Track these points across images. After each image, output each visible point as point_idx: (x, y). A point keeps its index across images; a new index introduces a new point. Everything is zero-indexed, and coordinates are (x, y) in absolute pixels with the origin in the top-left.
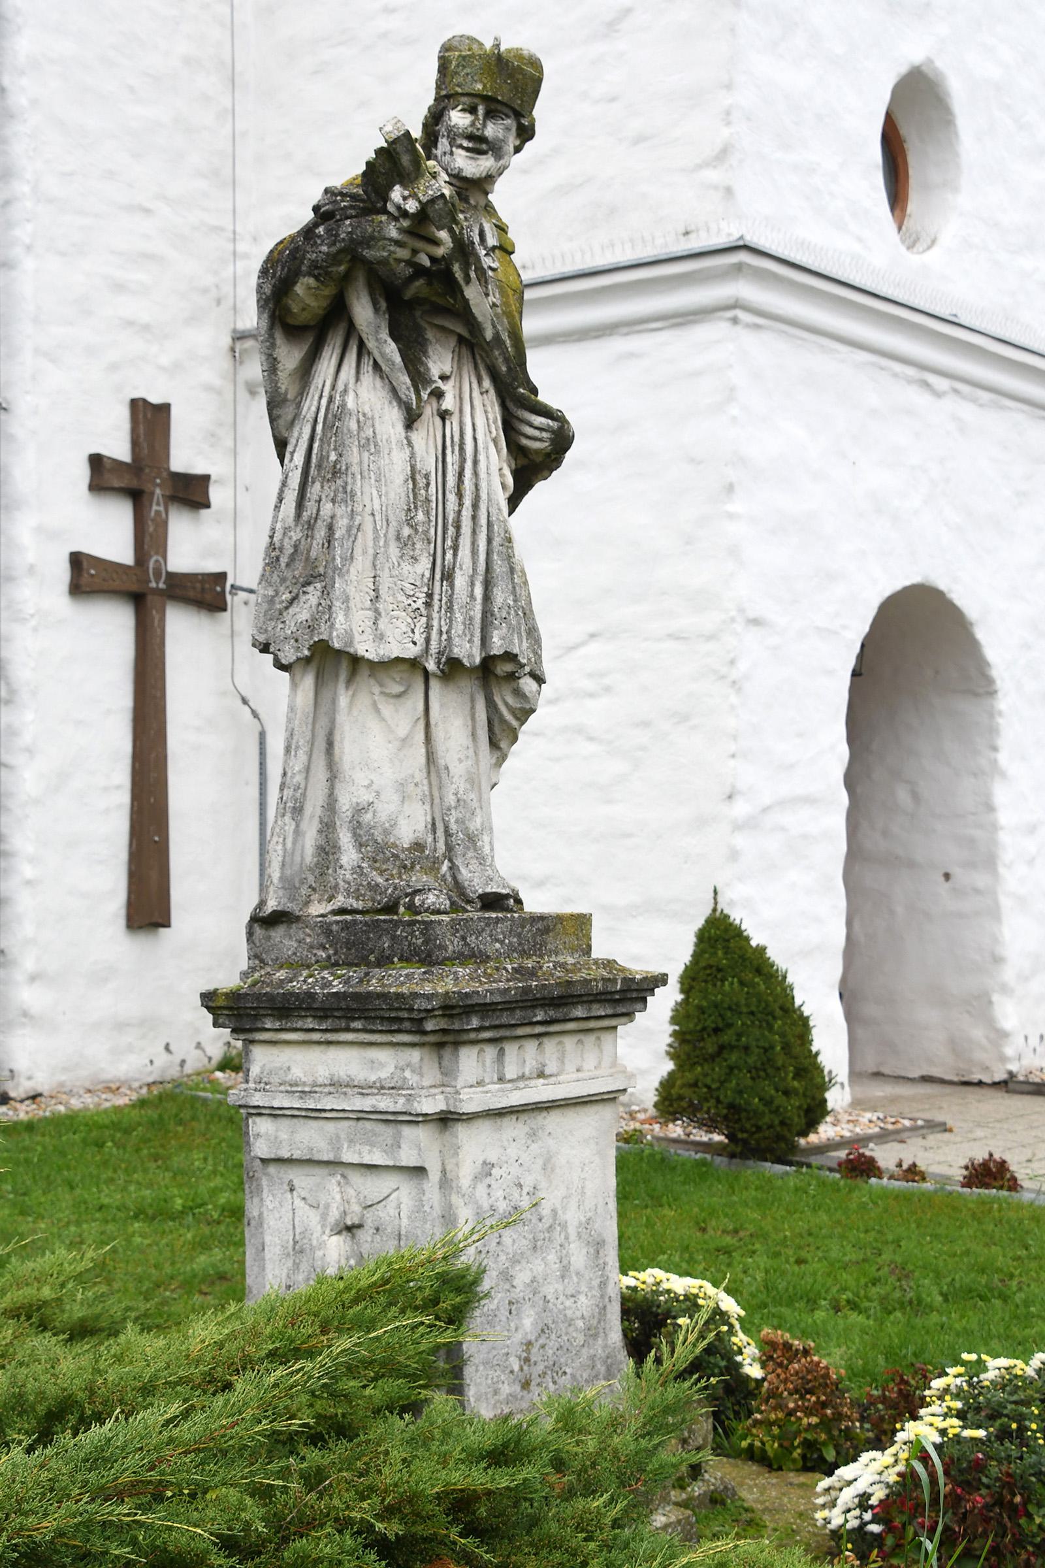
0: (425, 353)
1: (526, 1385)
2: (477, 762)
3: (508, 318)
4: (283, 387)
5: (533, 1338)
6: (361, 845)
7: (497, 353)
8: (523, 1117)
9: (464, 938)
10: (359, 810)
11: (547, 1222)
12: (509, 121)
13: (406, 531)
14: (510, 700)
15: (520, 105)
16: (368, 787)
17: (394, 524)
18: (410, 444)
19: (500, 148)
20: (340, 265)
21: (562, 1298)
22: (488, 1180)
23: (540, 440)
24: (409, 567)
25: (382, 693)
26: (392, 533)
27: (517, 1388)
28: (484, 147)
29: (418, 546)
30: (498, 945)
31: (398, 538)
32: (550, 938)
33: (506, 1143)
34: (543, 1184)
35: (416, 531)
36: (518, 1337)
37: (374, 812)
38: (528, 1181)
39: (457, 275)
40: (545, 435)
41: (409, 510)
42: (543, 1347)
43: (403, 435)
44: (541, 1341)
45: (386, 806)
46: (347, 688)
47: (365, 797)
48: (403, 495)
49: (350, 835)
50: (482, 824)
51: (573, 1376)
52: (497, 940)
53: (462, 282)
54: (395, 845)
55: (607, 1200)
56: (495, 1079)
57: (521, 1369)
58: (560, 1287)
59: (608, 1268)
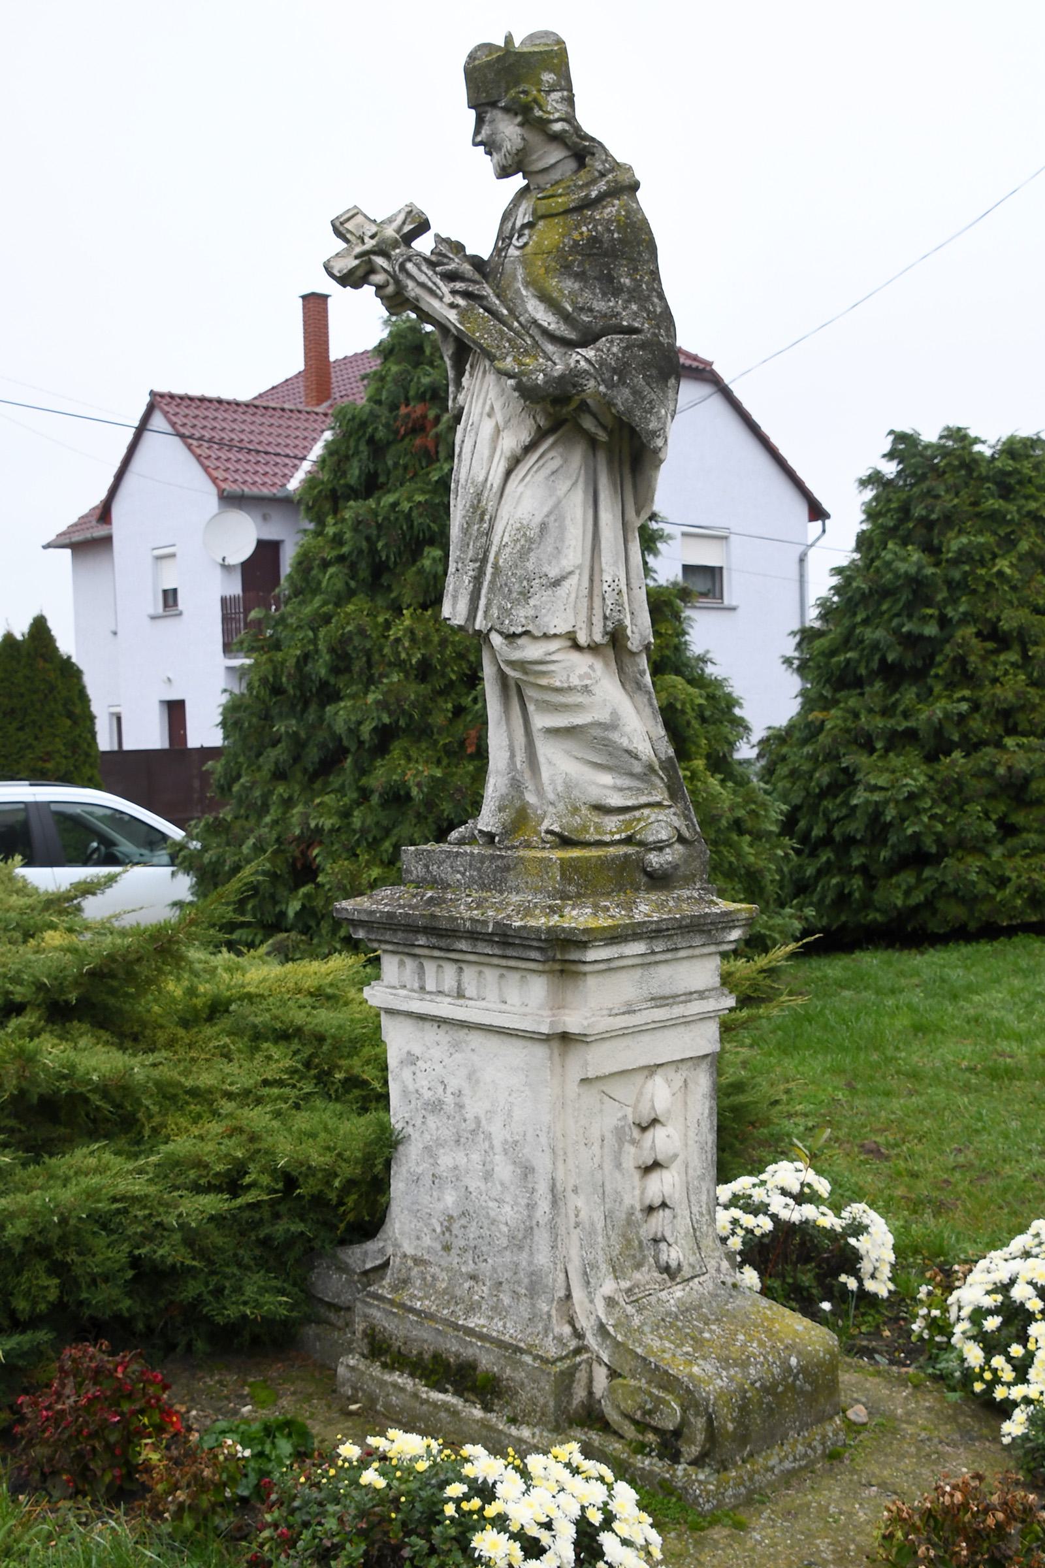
1: (447, 1248)
8: (444, 1027)
9: (426, 866)
30: (459, 876)
32: (511, 876)
34: (467, 1091)
36: (440, 1206)
38: (454, 1083)
51: (494, 1269)
58: (483, 1187)
59: (537, 1195)
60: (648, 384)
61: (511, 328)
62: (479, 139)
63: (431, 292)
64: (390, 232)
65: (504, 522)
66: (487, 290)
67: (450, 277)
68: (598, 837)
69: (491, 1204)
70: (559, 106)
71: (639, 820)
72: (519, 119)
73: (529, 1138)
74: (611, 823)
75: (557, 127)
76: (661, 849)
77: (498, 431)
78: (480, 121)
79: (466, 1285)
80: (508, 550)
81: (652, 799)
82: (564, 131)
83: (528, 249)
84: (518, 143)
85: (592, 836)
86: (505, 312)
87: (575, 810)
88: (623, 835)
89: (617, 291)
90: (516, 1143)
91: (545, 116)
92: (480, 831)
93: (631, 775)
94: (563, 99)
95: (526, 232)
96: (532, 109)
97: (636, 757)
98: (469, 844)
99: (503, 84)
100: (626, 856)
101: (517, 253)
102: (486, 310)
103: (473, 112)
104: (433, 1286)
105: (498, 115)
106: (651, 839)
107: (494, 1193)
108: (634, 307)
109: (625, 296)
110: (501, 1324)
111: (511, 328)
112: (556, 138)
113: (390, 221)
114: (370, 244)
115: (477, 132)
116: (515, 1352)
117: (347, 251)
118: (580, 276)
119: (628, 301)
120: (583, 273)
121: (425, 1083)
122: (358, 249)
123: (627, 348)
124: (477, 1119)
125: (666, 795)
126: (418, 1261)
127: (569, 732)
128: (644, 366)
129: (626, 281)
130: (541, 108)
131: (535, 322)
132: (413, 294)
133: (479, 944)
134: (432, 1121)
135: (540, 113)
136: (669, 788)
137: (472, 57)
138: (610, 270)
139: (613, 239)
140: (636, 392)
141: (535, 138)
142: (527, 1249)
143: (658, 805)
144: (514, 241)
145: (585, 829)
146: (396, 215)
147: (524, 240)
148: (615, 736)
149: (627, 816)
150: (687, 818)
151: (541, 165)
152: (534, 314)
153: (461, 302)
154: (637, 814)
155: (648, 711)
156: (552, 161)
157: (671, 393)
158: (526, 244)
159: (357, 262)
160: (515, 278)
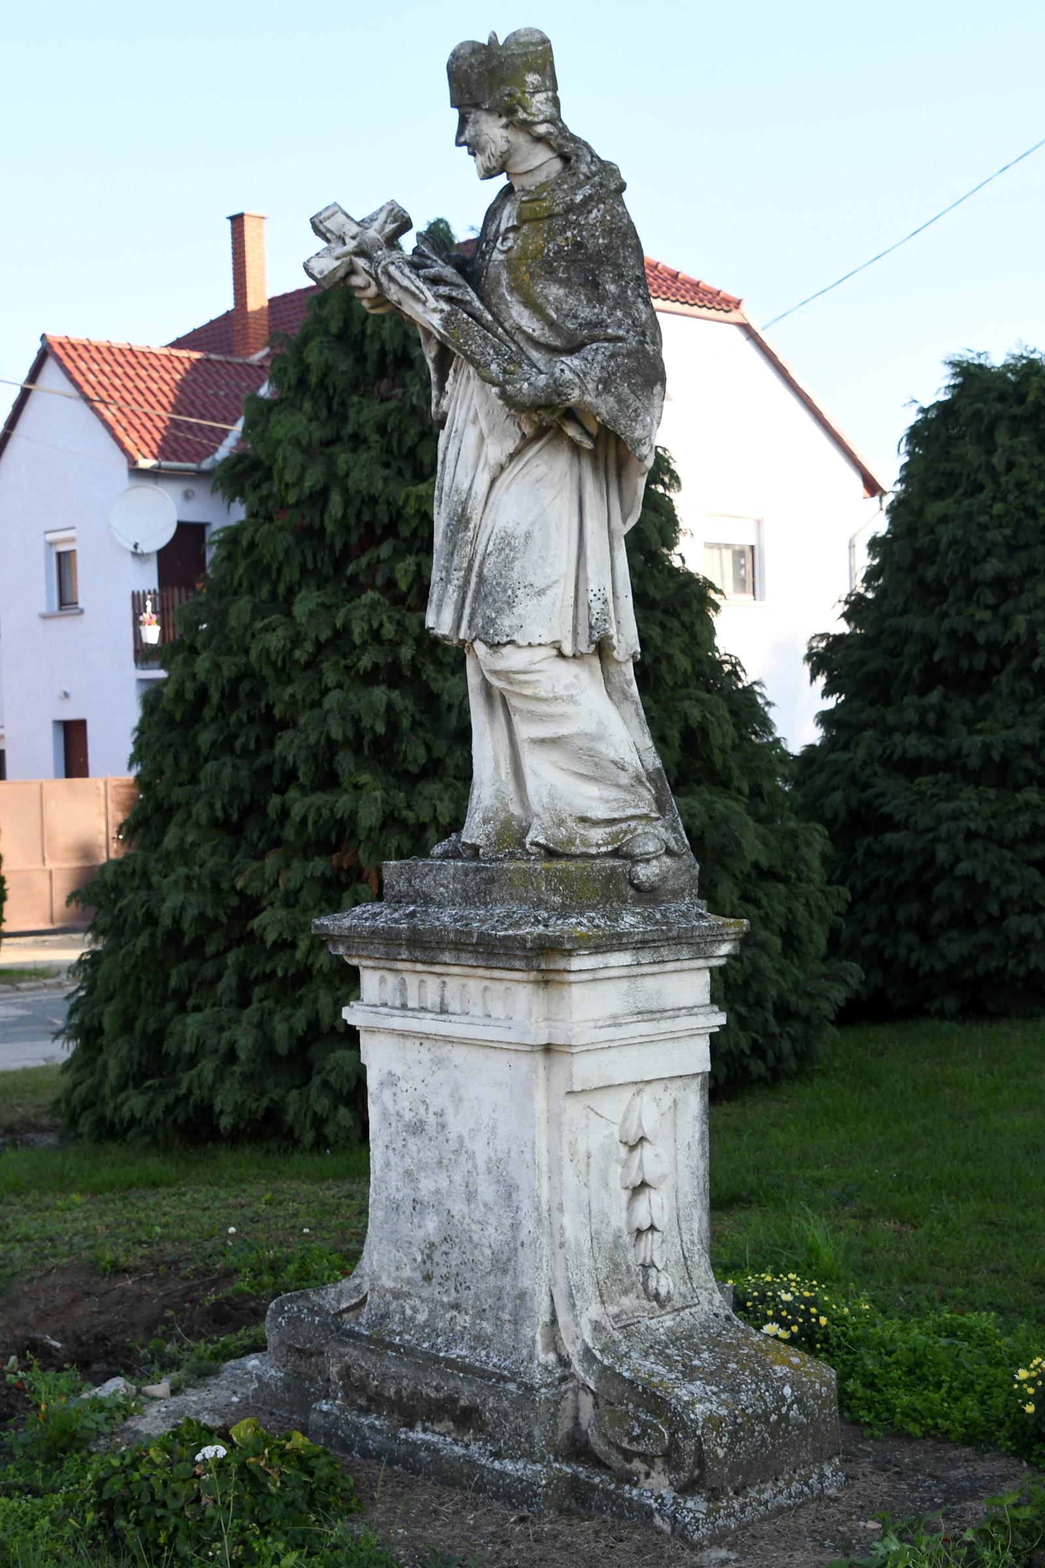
1: (428, 1278)
5: (437, 1241)
11: (454, 1145)
19: (478, 143)
21: (467, 1220)
22: (394, 1089)
27: (417, 1276)
32: (495, 888)
33: (410, 1063)
34: (450, 1111)
36: (420, 1234)
38: (436, 1104)
42: (446, 1254)
44: (445, 1248)
51: (477, 1297)
52: (442, 885)
55: (523, 1148)
56: (398, 1003)
57: (424, 1262)
58: (466, 1210)
59: (521, 1214)
60: (633, 392)
61: (495, 335)
62: (462, 139)
63: (414, 295)
64: (372, 233)
65: (488, 531)
66: (471, 296)
67: (435, 281)
68: (584, 850)
69: (474, 1227)
70: (543, 108)
71: (626, 833)
72: (504, 120)
73: (513, 1155)
74: (597, 835)
75: (542, 129)
76: (648, 861)
77: (482, 439)
78: (463, 122)
79: (448, 1316)
80: (492, 559)
81: (638, 812)
82: (551, 133)
83: (513, 254)
84: (503, 146)
85: (578, 849)
86: (490, 318)
87: (561, 823)
88: (610, 849)
89: (601, 300)
90: (500, 1160)
91: (530, 118)
92: (464, 844)
93: (618, 786)
94: (547, 99)
95: (511, 235)
96: (516, 111)
97: (623, 769)
98: (454, 858)
100: (613, 868)
101: (502, 257)
102: (470, 315)
103: (456, 111)
104: (412, 1319)
105: (483, 117)
106: (637, 851)
107: (477, 1216)
108: (619, 314)
109: (611, 303)
110: (484, 1353)
111: (495, 335)
112: (539, 139)
113: (372, 219)
115: (461, 132)
116: (498, 1381)
117: (328, 249)
118: (566, 283)
119: (614, 308)
120: (568, 279)
121: (406, 1104)
122: (340, 250)
123: (613, 356)
124: (460, 1139)
125: (654, 807)
126: (397, 1295)
127: (553, 742)
128: (629, 374)
129: (612, 288)
130: (525, 110)
131: (519, 328)
132: (395, 298)
133: (463, 955)
134: (413, 1143)
135: (525, 115)
136: (657, 800)
137: (455, 56)
138: (595, 276)
139: (598, 244)
140: (620, 401)
141: (521, 140)
142: (511, 1272)
143: (645, 817)
144: (498, 244)
145: (571, 841)
146: (377, 213)
147: (509, 243)
148: (602, 747)
149: (614, 829)
150: (675, 830)
152: (518, 319)
153: (446, 307)
154: (624, 826)
155: (636, 721)
156: (537, 163)
157: (656, 400)
158: (510, 249)
159: (338, 263)
160: (499, 283)
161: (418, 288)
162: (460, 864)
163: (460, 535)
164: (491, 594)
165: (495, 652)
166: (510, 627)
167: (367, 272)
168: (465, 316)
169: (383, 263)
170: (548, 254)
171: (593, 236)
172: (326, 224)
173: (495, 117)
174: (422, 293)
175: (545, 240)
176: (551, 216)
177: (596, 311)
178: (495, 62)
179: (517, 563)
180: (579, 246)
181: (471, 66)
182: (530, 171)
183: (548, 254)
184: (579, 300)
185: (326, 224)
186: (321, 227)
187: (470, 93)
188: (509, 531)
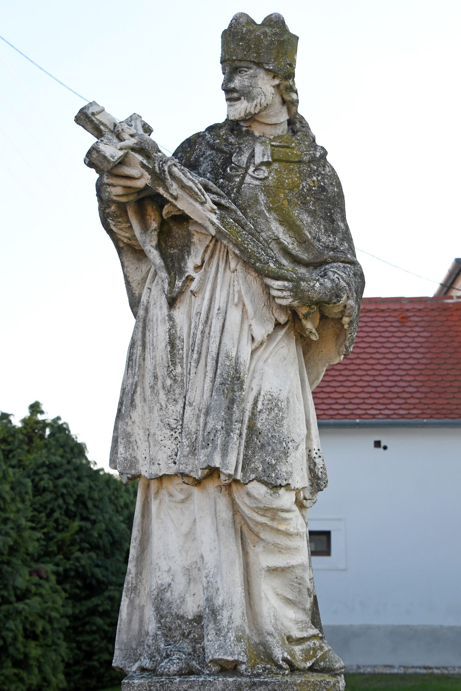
0: (189, 253)
2: (220, 551)
3: (275, 211)
4: (137, 293)
6: (162, 617)
7: (225, 242)
10: (162, 590)
12: (251, 71)
13: (169, 382)
14: (247, 500)
15: (256, 57)
16: (169, 570)
17: (160, 378)
18: (171, 318)
19: (249, 92)
20: (110, 207)
23: (283, 298)
24: (173, 408)
25: (171, 501)
26: (160, 384)
28: (235, 95)
29: (177, 391)
31: (164, 388)
35: (175, 381)
37: (171, 591)
39: (165, 196)
40: (285, 294)
41: (169, 366)
43: (167, 313)
45: (178, 586)
46: (155, 498)
47: (167, 579)
48: (165, 356)
49: (153, 609)
50: (223, 601)
53: (171, 199)
54: (181, 617)
72: (277, 82)
80: (264, 416)
99: (274, 52)
101: (257, 183)
105: (262, 74)
114: (131, 142)
118: (312, 214)
120: (315, 211)
138: (331, 213)
151: (274, 120)
158: (266, 178)
160: (257, 201)
161: (200, 190)
162: (231, 680)
163: (237, 394)
164: (269, 444)
165: (275, 493)
166: (287, 473)
167: (143, 166)
168: (232, 220)
169: (169, 163)
170: (302, 189)
171: (332, 184)
172: (98, 117)
173: (271, 78)
174: (203, 195)
175: (299, 178)
176: (300, 162)
177: (331, 239)
178: (286, 37)
179: (285, 421)
180: (323, 189)
181: (265, 34)
182: (275, 124)
183: (302, 189)
184: (319, 229)
185: (98, 117)
186: (94, 119)
187: (257, 53)
188: (274, 395)
